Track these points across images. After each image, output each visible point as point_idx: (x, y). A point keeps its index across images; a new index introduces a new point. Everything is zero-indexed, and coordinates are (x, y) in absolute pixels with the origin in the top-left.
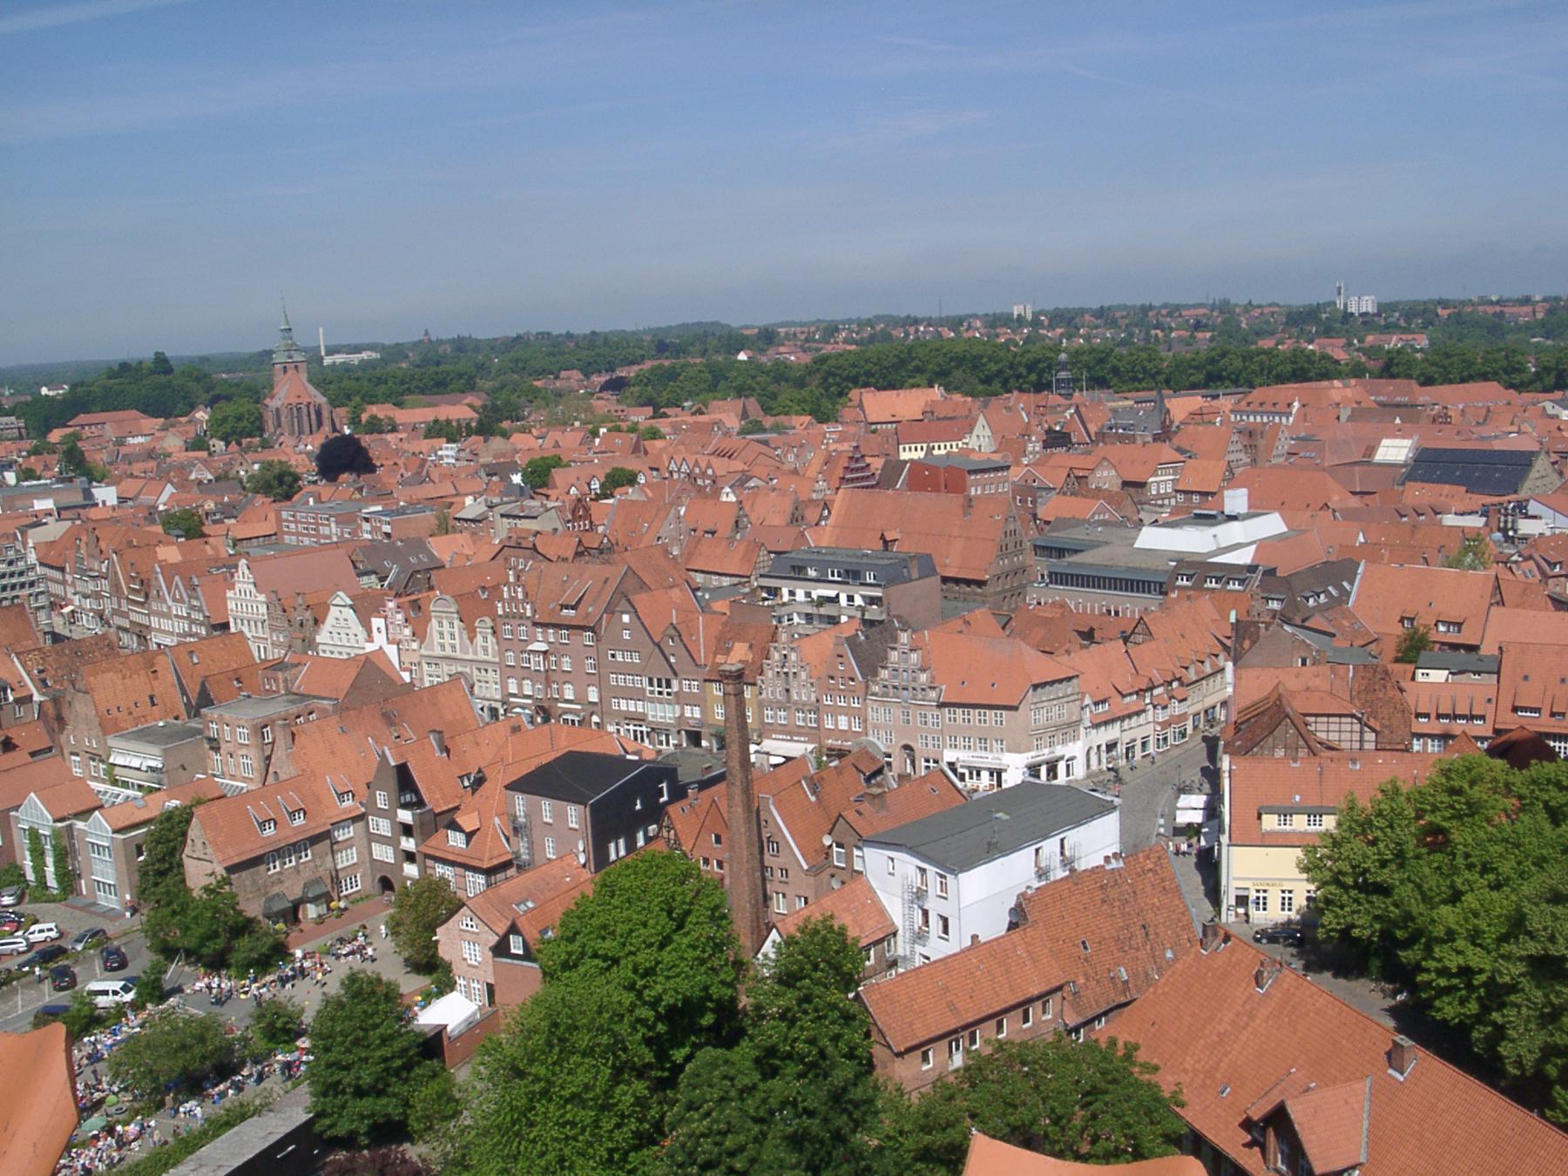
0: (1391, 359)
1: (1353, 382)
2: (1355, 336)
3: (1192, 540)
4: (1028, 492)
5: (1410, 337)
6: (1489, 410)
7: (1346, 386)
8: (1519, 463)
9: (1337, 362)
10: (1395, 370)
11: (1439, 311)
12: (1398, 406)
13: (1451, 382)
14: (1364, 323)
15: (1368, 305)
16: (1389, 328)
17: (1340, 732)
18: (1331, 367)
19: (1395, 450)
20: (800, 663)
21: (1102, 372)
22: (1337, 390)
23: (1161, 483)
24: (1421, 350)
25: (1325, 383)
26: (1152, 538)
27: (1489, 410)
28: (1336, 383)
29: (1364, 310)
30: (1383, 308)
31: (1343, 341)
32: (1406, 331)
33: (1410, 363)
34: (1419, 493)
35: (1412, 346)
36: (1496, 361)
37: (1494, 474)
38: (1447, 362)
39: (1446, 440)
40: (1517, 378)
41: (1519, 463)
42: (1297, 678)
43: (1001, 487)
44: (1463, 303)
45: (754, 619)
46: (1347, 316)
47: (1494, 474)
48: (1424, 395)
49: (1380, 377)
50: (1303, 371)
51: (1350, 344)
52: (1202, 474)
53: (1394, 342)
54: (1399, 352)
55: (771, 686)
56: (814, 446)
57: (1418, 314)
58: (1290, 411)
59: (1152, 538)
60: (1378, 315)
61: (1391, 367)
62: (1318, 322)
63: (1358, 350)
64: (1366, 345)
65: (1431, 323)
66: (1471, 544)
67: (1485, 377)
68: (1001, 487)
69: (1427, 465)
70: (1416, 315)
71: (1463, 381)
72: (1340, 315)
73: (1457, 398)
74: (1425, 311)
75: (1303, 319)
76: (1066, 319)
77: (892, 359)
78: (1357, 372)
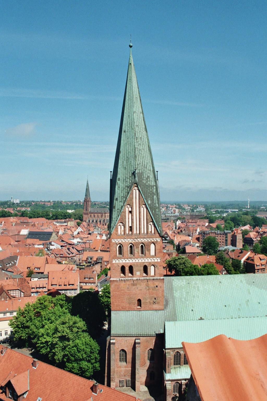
0: (23, 213)
1: (15, 217)
2: (15, 208)
5: (27, 208)
6: (43, 223)
7: (14, 218)
8: (50, 234)
9: (12, 213)
10: (24, 215)
11: (33, 203)
12: (25, 223)
13: (35, 218)
14: (17, 205)
15: (18, 201)
16: (22, 206)
18: (11, 214)
19: (25, 232)
22: (12, 219)
24: (29, 211)
25: (9, 218)
27: (43, 223)
28: (12, 218)
29: (17, 202)
30: (21, 202)
31: (13, 209)
32: (26, 207)
33: (27, 213)
34: (30, 241)
35: (27, 210)
36: (44, 213)
38: (34, 214)
39: (35, 230)
40: (48, 217)
41: (50, 234)
44: (37, 202)
46: (13, 204)
47: (45, 237)
48: (30, 220)
49: (21, 216)
51: (14, 209)
53: (23, 209)
54: (25, 211)
57: (28, 204)
60: (20, 203)
61: (23, 215)
62: (7, 205)
63: (16, 211)
64: (18, 210)
65: (31, 205)
66: (41, 251)
67: (42, 217)
69: (32, 235)
70: (28, 204)
71: (38, 217)
72: (12, 203)
74: (30, 203)
78: (16, 215)
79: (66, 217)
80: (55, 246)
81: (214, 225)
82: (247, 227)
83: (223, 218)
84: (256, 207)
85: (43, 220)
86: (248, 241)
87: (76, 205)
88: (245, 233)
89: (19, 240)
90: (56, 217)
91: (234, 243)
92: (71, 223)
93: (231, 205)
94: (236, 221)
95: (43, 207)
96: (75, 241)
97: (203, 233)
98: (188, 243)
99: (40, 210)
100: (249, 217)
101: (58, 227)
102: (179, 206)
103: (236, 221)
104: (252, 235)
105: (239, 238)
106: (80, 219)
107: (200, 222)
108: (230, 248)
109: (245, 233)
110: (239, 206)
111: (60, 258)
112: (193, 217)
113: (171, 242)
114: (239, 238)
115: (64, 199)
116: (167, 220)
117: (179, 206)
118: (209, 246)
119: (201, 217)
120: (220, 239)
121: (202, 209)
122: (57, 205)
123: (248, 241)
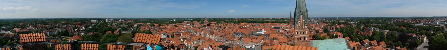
4: (251, 29)
8: (280, 28)
19: (273, 27)
20: (236, 39)
23: (259, 29)
37: (278, 28)
41: (280, 28)
45: (233, 37)
47: (278, 28)
50: (268, 22)
52: (261, 28)
55: (234, 41)
56: (237, 26)
58: (266, 25)
61: (273, 22)
69: (275, 28)
73: (276, 24)
75: (268, 19)
79: (285, 22)
85: (278, 23)
86: (337, 29)
87: (288, 19)
88: (336, 26)
89: (271, 29)
90: (282, 23)
91: (333, 29)
92: (286, 24)
93: (333, 18)
94: (334, 23)
97: (324, 27)
98: (319, 30)
99: (277, 21)
101: (283, 25)
102: (318, 19)
104: (338, 27)
105: (334, 28)
106: (288, 23)
107: (323, 23)
108: (332, 31)
109: (336, 26)
110: (335, 18)
111: (282, 34)
112: (321, 22)
113: (315, 30)
114: (334, 28)
115: (284, 17)
116: (314, 23)
118: (326, 31)
119: (324, 22)
120: (329, 28)
121: (324, 20)
122: (282, 19)
123: (337, 29)
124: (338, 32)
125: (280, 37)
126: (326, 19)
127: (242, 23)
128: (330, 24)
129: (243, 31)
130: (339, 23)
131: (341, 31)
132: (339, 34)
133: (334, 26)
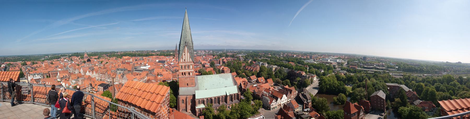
3: (144, 68)
8: (165, 61)
17: (153, 81)
19: (157, 61)
21: (139, 55)
22: (154, 56)
26: (142, 67)
34: (159, 64)
37: (163, 62)
39: (160, 60)
41: (165, 61)
42: (151, 77)
43: (132, 64)
47: (163, 62)
57: (159, 51)
59: (142, 67)
61: (157, 55)
66: (162, 67)
68: (132, 64)
69: (159, 62)
73: (161, 57)
76: (137, 51)
77: (126, 54)
79: (170, 55)
80: (166, 65)
81: (214, 57)
82: (224, 58)
83: (217, 55)
84: (227, 51)
85: (163, 57)
86: (224, 62)
87: (173, 51)
88: (223, 60)
89: (156, 63)
90: (167, 55)
91: (219, 63)
92: (171, 58)
93: (220, 50)
94: (221, 56)
95: (164, 52)
96: (172, 63)
97: (211, 60)
98: (206, 64)
99: (162, 53)
100: (225, 54)
101: (167, 59)
103: (221, 56)
104: (225, 60)
105: (221, 61)
107: (210, 56)
108: (218, 65)
109: (223, 60)
111: (167, 69)
112: (209, 55)
113: (201, 63)
114: (221, 61)
116: (200, 56)
117: (205, 51)
119: (211, 55)
120: (215, 62)
122: (168, 51)
123: (224, 62)
124: (225, 66)
125: (165, 73)
126: (213, 51)
127: (125, 57)
128: (216, 57)
129: (126, 66)
130: (227, 56)
131: (228, 66)
132: (226, 69)
133: (221, 59)
